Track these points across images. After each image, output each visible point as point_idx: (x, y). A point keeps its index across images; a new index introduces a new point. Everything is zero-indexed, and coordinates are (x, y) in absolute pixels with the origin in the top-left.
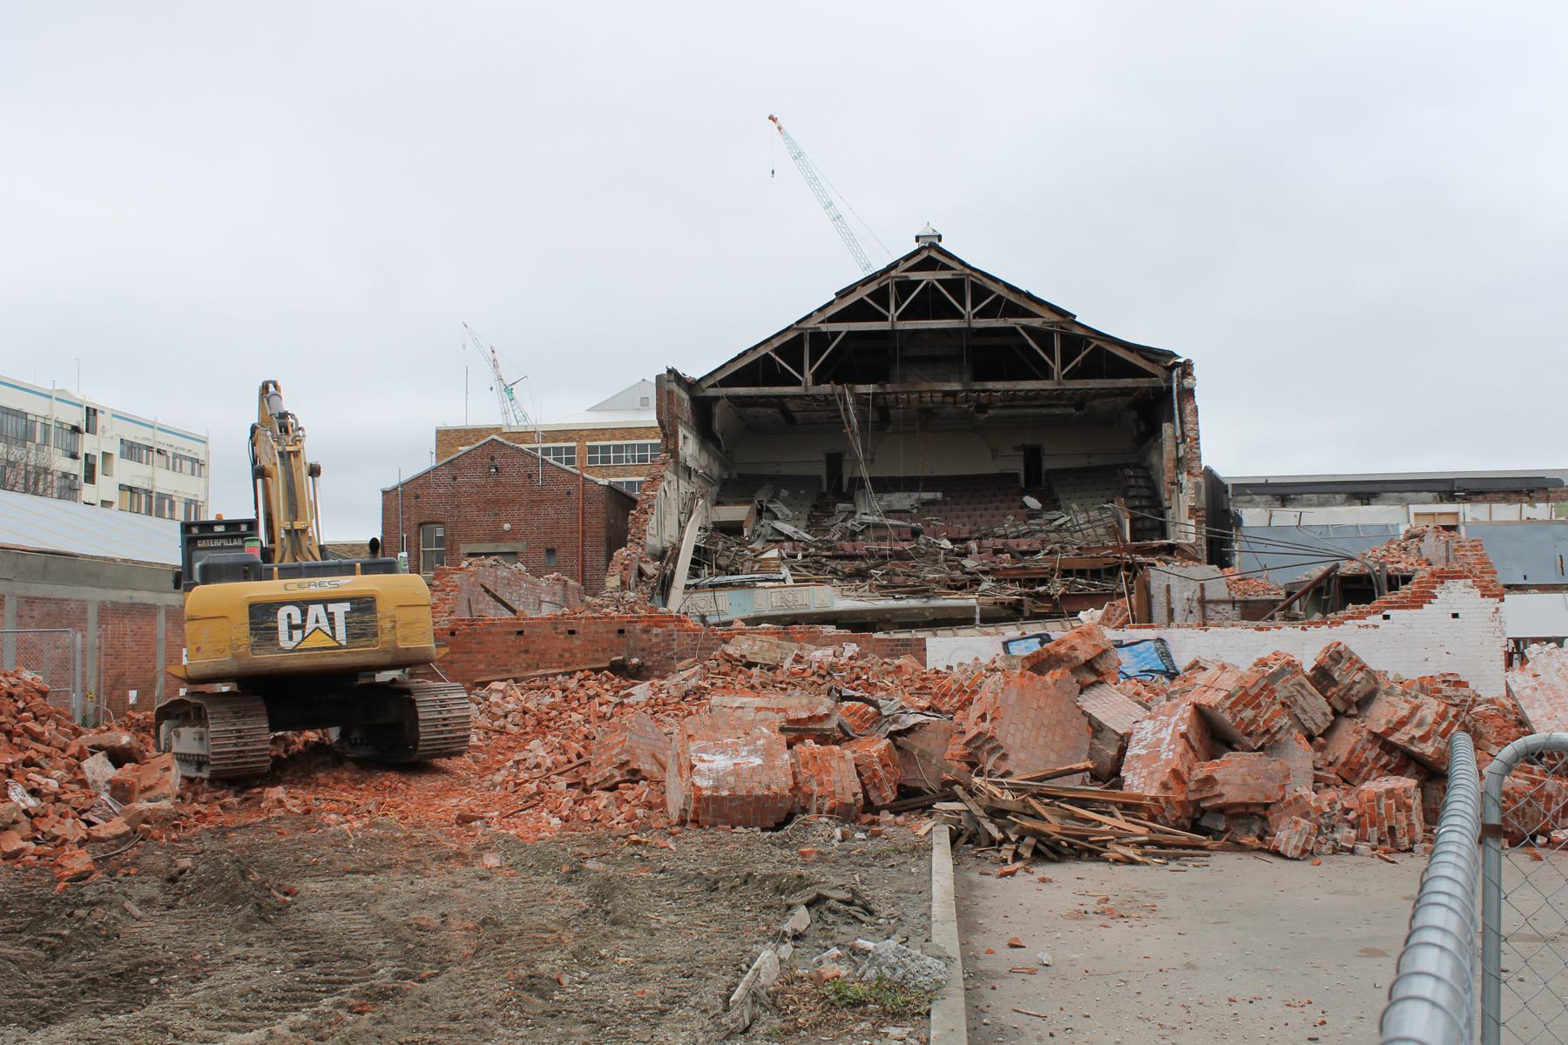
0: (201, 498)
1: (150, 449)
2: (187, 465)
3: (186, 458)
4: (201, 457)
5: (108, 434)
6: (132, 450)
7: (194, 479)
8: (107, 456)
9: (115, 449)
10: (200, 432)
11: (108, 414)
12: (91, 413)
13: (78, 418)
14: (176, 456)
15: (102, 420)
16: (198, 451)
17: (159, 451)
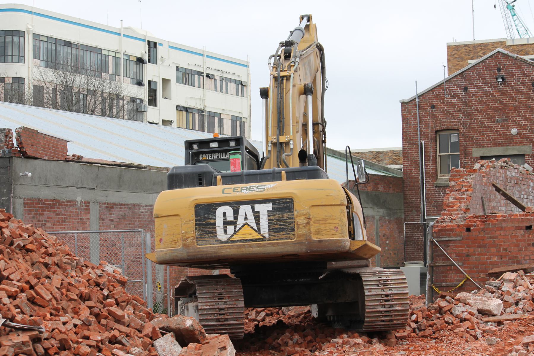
0: (245, 115)
1: (200, 74)
2: (232, 86)
3: (231, 80)
4: (244, 79)
5: (166, 63)
6: (186, 76)
7: (239, 99)
8: (165, 81)
9: (172, 75)
10: (241, 57)
11: (166, 45)
12: (152, 45)
13: (141, 51)
14: (222, 79)
15: (160, 51)
16: (240, 74)
17: (208, 76)
